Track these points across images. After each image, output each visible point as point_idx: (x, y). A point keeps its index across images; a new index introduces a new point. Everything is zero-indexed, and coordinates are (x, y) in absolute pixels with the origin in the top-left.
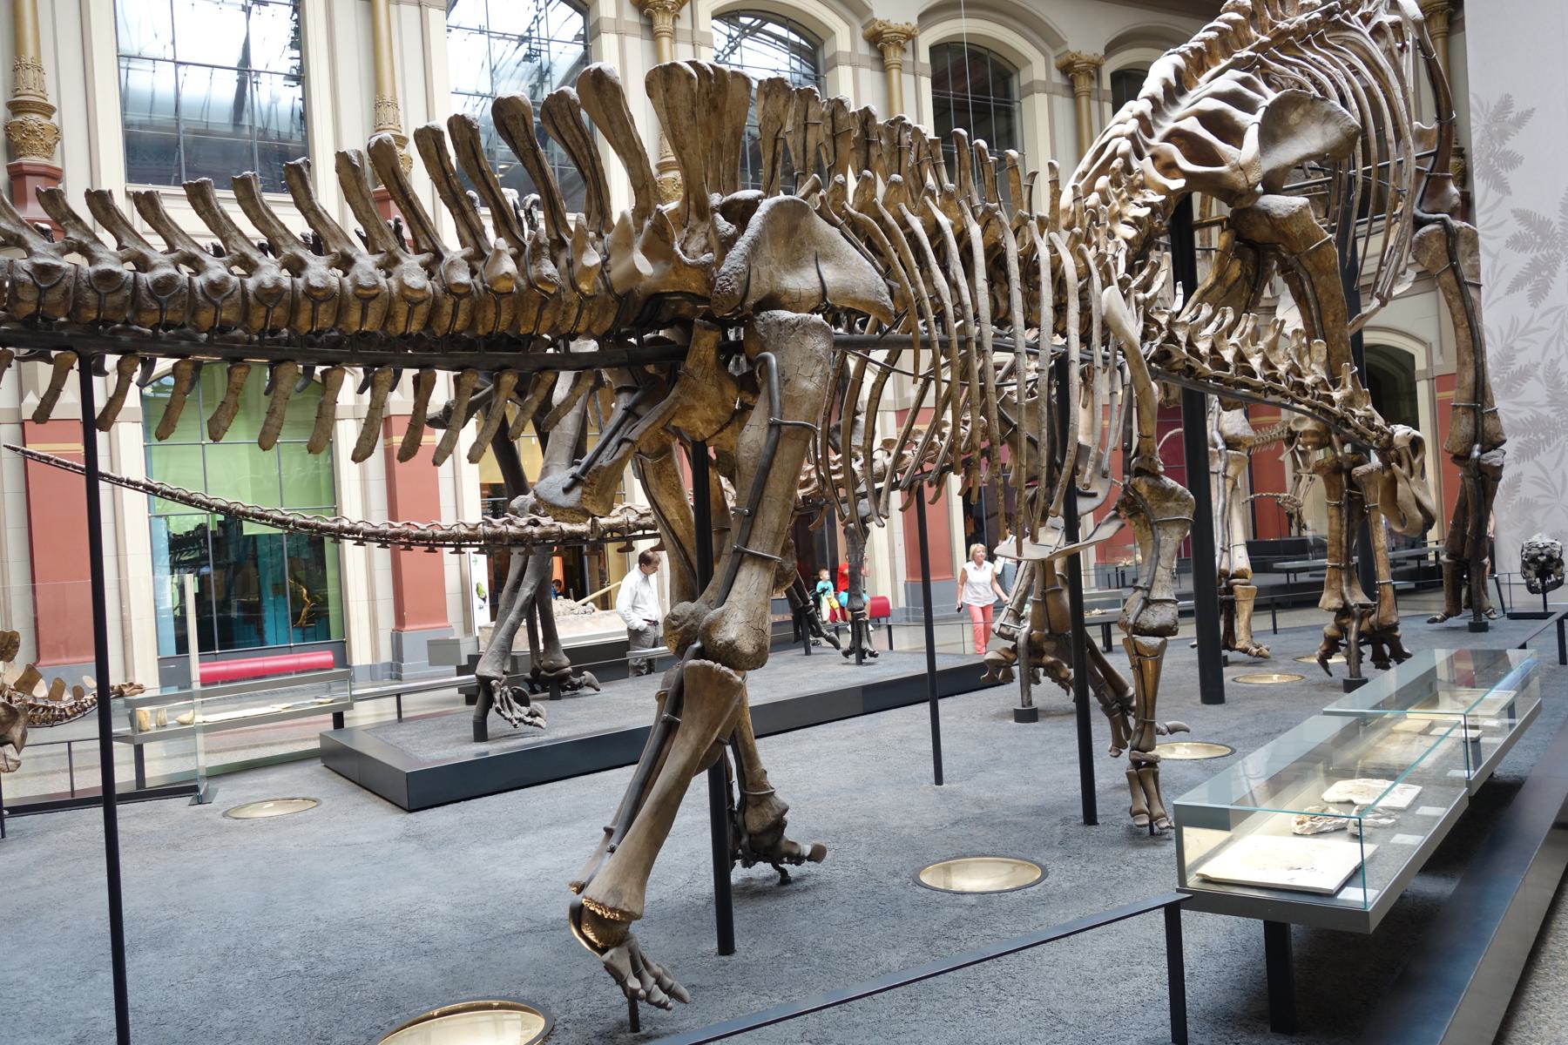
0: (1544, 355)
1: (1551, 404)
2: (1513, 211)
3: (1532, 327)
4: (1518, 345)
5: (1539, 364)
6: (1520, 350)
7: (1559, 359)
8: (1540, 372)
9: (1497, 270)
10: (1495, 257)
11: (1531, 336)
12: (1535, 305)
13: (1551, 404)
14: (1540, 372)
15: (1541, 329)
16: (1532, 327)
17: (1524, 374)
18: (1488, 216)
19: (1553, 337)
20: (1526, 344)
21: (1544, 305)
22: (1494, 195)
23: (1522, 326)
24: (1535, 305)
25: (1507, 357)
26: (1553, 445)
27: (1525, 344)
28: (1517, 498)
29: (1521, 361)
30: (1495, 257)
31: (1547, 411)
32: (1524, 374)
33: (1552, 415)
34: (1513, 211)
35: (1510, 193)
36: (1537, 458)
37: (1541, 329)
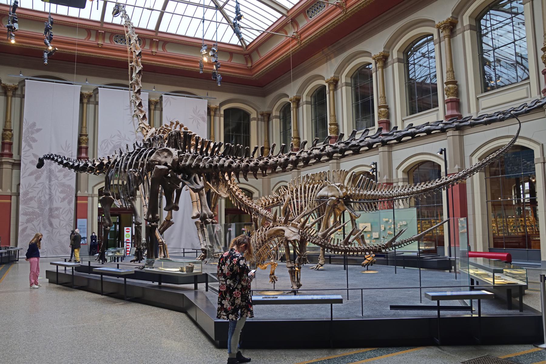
0: (38, 194)
1: (38, 208)
2: (33, 154)
3: (35, 186)
4: (30, 190)
5: (36, 197)
6: (32, 192)
7: (42, 197)
8: (36, 199)
9: (26, 168)
10: (26, 165)
11: (34, 189)
12: (36, 181)
13: (38, 208)
14: (36, 199)
15: (38, 187)
16: (35, 186)
17: (31, 199)
18: (25, 153)
19: (40, 191)
20: (32, 191)
21: (39, 181)
22: (27, 148)
23: (32, 185)
24: (36, 181)
25: (26, 193)
26: (38, 219)
27: (32, 191)
28: (25, 233)
29: (30, 195)
30: (26, 165)
31: (37, 210)
32: (31, 199)
33: (38, 211)
34: (33, 154)
35: (33, 149)
36: (33, 223)
37: (38, 187)
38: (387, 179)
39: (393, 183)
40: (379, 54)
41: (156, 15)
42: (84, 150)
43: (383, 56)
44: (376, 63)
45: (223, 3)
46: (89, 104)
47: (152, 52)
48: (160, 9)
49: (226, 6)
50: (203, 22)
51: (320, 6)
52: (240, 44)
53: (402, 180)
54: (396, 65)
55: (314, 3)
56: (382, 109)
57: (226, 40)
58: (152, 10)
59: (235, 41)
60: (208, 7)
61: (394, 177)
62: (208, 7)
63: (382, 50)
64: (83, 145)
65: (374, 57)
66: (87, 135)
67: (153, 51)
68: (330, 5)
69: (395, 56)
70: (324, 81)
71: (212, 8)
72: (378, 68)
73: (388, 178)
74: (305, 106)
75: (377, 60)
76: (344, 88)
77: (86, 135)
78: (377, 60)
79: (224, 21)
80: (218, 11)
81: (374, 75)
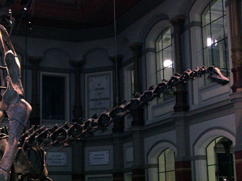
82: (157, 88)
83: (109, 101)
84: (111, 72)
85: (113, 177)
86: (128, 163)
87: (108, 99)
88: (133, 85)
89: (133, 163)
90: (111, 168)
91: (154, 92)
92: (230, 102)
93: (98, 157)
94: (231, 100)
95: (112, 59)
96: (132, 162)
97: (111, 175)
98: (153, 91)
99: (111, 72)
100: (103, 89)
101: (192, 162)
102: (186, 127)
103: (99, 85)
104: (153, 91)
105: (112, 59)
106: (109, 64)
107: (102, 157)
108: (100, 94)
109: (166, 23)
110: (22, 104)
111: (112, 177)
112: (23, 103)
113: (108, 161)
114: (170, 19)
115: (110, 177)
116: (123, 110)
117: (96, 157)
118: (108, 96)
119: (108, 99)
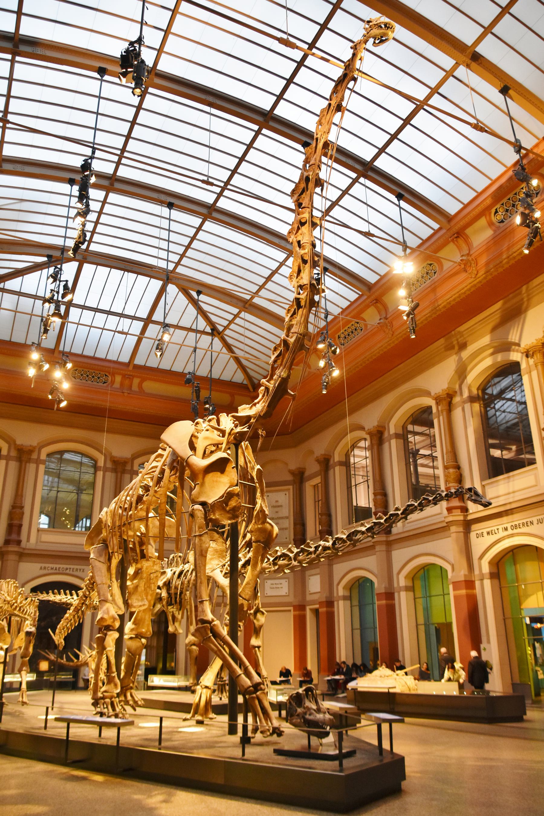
38: (465, 575)
39: (474, 581)
40: (441, 391)
41: (132, 341)
42: (15, 529)
43: (448, 394)
44: (437, 404)
45: (223, 328)
46: (29, 463)
47: (123, 393)
48: (138, 333)
49: (227, 332)
50: (195, 351)
51: (356, 330)
52: (245, 382)
53: (488, 576)
54: (467, 406)
55: (348, 324)
56: (451, 470)
57: (226, 377)
58: (126, 334)
59: (239, 377)
60: (203, 332)
61: (477, 572)
62: (203, 332)
63: (445, 386)
64: (16, 522)
65: (435, 396)
66: (23, 507)
67: (124, 391)
68: (369, 327)
69: (466, 394)
70: (364, 433)
71: (207, 334)
72: (440, 412)
73: (467, 573)
74: (337, 469)
75: (438, 400)
76: (393, 442)
77: (22, 507)
78: (438, 400)
79: (224, 350)
80: (216, 340)
81: (436, 422)
82: (405, 510)
83: (287, 520)
84: (291, 487)
85: (294, 611)
86: (311, 594)
87: (287, 518)
88: (320, 502)
89: (319, 594)
90: (291, 599)
91: (402, 514)
92: (445, 524)
93: (275, 586)
94: (447, 523)
95: (292, 473)
96: (319, 592)
97: (292, 608)
98: (399, 512)
99: (291, 487)
100: (281, 506)
101: (396, 595)
102: (389, 553)
103: (277, 501)
104: (399, 512)
105: (292, 473)
106: (289, 478)
107: (279, 586)
108: (277, 512)
109: (363, 434)
110: (268, 525)
111: (292, 610)
112: (270, 524)
113: (287, 592)
114: (366, 429)
115: (290, 611)
116: (363, 533)
117: (272, 586)
118: (287, 515)
119: (287, 518)
